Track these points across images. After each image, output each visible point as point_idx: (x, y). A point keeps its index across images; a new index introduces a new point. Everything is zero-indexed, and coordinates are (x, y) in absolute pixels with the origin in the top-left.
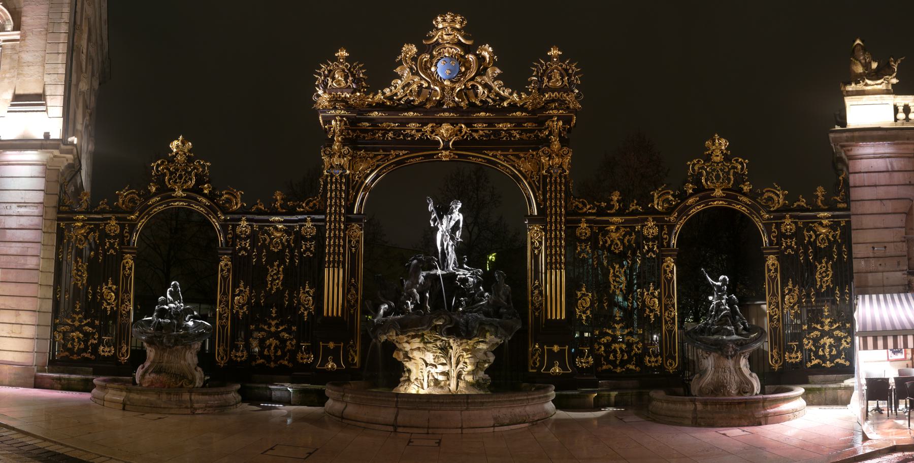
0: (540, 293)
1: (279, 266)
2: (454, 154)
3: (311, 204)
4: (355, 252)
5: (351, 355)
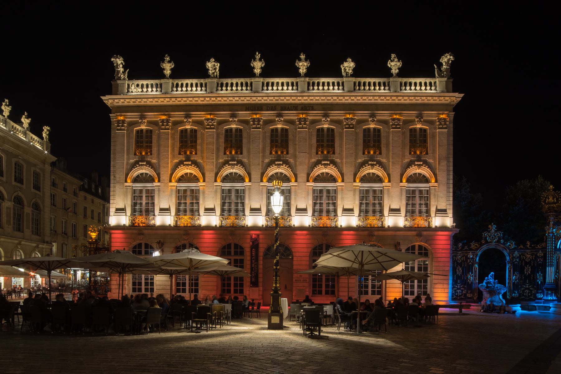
1: (529, 266)
3: (541, 246)
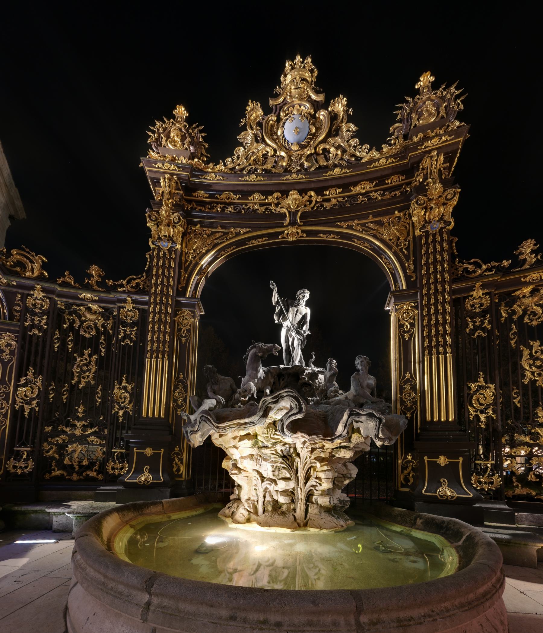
0: (414, 388)
1: (90, 356)
2: (303, 231)
3: (134, 283)
4: (186, 343)
5: (177, 464)
